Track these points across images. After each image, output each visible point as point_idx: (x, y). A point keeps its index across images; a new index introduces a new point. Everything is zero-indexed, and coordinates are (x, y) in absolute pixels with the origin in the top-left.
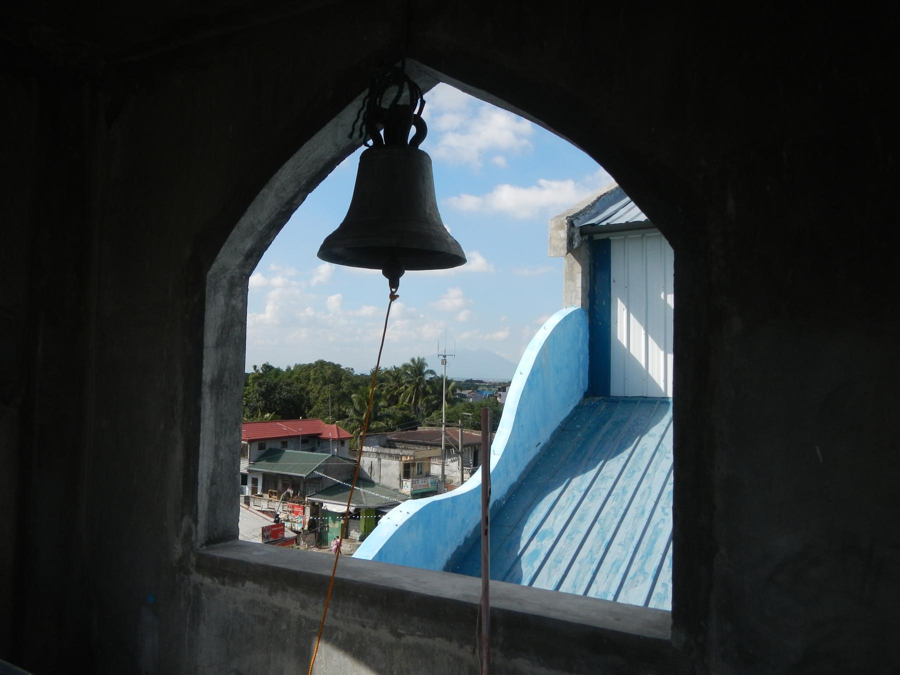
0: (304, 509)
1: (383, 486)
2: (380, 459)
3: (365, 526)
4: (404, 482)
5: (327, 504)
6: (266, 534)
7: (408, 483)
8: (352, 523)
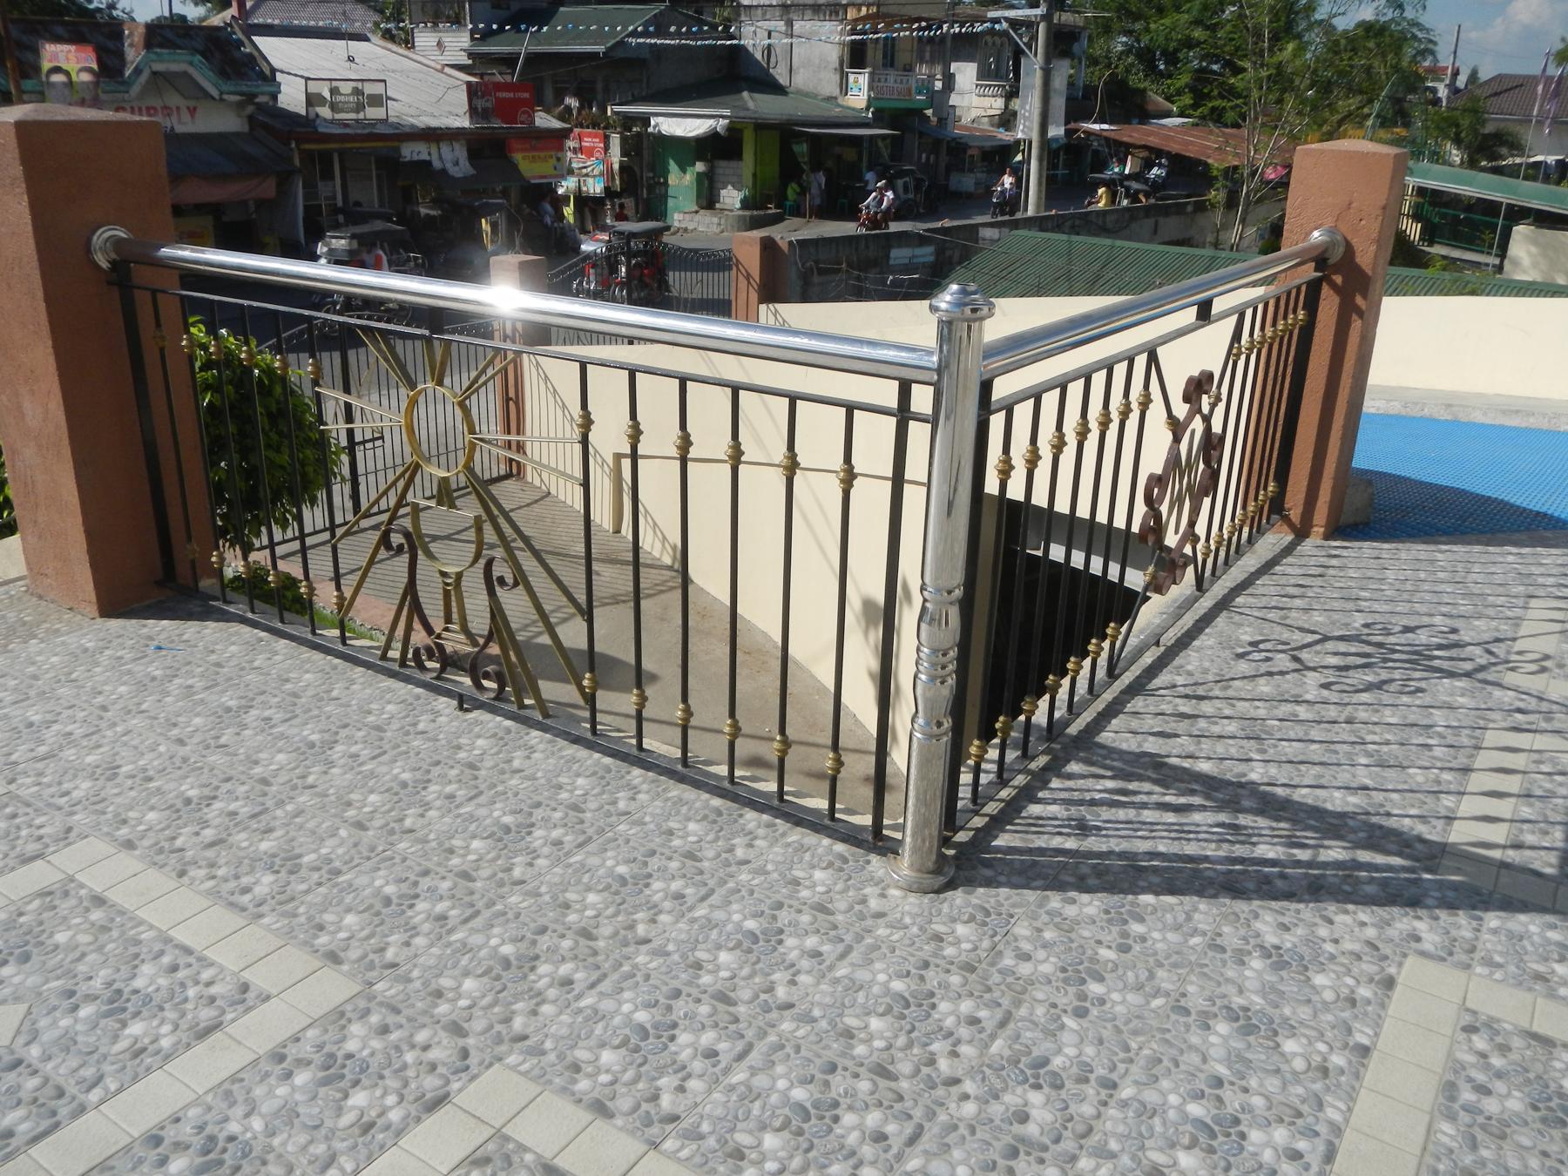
0: (606, 139)
1: (799, 92)
2: (790, 24)
3: (755, 175)
4: (852, 78)
5: (660, 119)
6: (480, 104)
7: (861, 78)
8: (724, 167)
